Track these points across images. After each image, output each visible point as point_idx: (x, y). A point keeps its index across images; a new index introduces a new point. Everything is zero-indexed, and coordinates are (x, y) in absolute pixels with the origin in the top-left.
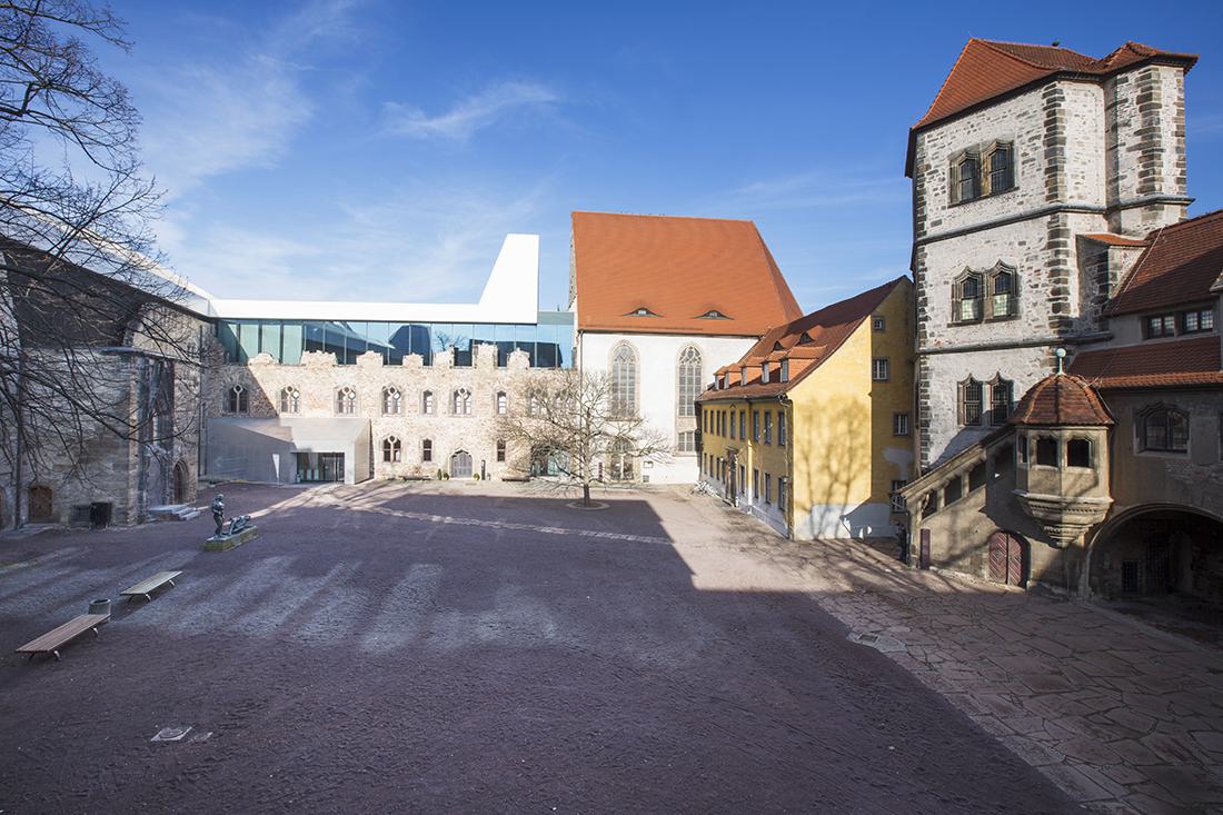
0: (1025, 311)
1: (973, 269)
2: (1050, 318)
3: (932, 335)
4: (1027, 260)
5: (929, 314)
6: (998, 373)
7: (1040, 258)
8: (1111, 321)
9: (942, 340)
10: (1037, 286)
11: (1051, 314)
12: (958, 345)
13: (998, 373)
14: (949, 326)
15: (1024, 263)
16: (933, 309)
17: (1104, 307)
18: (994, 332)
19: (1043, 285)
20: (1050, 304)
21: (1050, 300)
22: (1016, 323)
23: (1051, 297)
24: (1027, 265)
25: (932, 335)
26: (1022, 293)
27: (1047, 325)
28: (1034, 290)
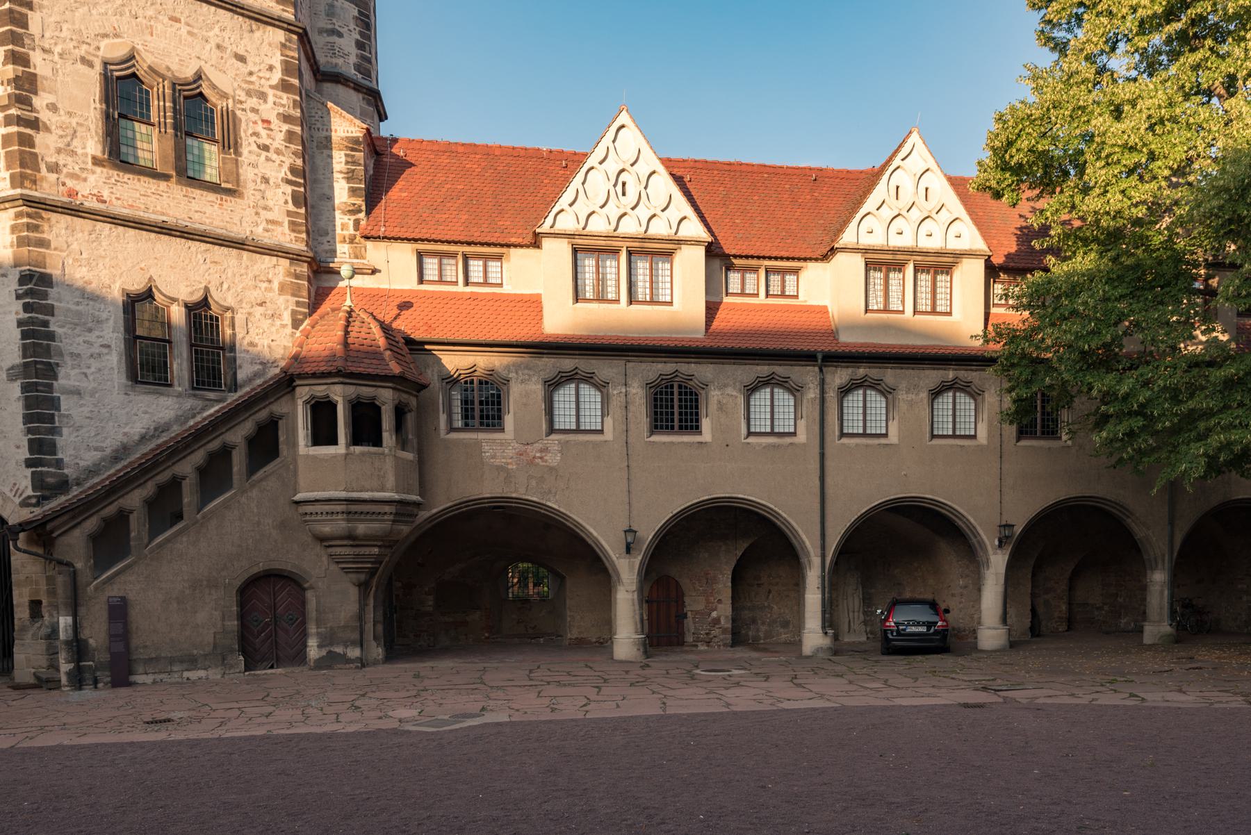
0: (251, 185)
1: (146, 60)
2: (289, 213)
3: (54, 168)
4: (249, 93)
5: (44, 116)
6: (207, 289)
7: (271, 99)
8: (369, 244)
9: (84, 189)
10: (266, 148)
11: (291, 207)
12: (119, 209)
13: (207, 289)
14: (96, 161)
15: (242, 96)
16: (53, 108)
17: (357, 222)
18: (195, 206)
19: (278, 152)
20: (289, 189)
21: (289, 182)
22: (230, 202)
23: (290, 177)
24: (253, 102)
25: (54, 168)
26: (245, 151)
27: (286, 224)
28: (264, 154)
